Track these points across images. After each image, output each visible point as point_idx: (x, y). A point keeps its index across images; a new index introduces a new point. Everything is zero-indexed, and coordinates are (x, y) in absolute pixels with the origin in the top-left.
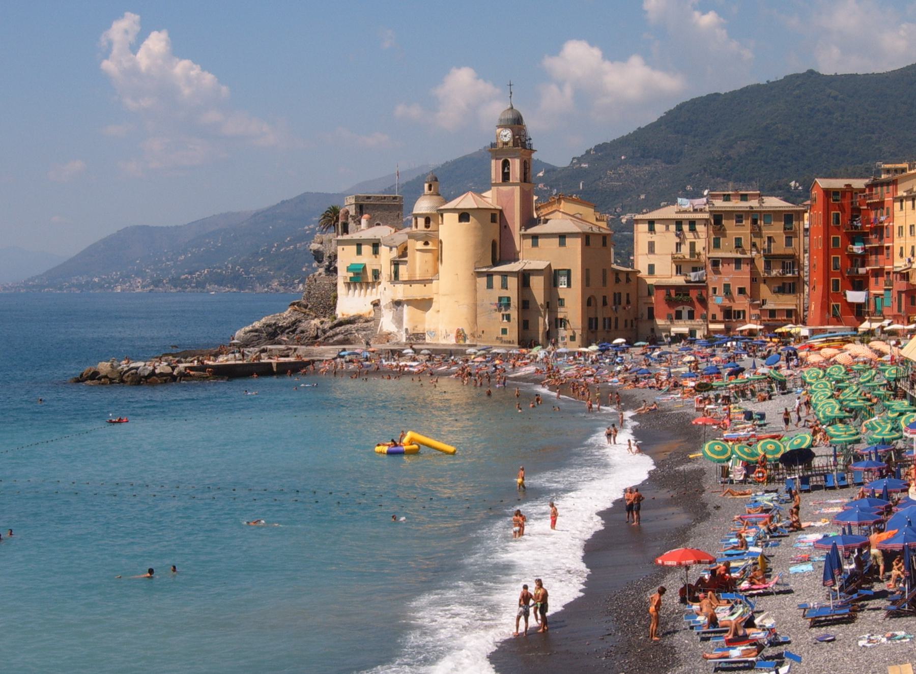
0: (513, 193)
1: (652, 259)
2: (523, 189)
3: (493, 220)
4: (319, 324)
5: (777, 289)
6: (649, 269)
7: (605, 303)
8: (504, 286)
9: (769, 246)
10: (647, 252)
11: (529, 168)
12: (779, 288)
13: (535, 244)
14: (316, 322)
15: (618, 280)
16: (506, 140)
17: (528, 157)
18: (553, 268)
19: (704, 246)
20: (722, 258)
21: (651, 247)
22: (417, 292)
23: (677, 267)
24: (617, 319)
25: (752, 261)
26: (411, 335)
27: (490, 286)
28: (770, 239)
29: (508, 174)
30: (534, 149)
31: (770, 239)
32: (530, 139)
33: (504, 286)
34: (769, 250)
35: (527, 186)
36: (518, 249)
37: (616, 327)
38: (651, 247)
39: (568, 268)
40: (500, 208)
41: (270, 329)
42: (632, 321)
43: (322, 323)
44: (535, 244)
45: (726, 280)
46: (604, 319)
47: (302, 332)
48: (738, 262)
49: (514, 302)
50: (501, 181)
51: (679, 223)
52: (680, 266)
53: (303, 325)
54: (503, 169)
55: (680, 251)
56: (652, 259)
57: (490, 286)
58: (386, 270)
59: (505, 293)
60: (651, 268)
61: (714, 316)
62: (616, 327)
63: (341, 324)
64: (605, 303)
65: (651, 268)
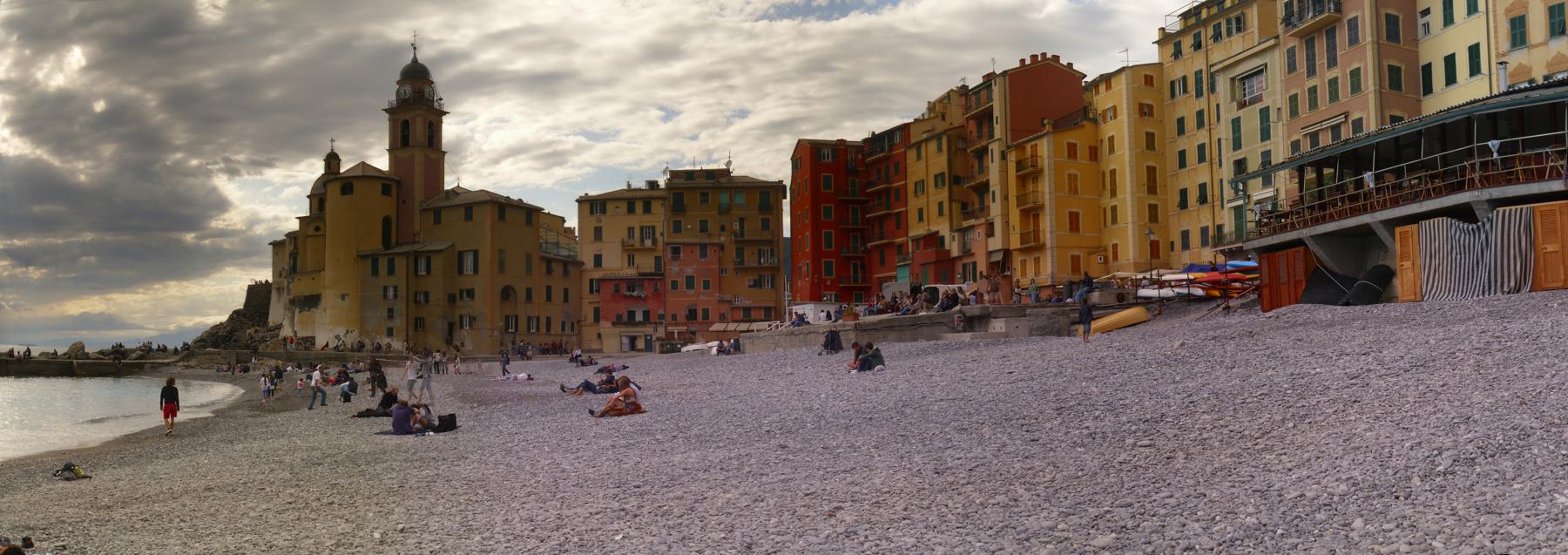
3: (386, 190)
5: (752, 283)
7: (529, 297)
8: (391, 271)
9: (742, 226)
10: (593, 239)
12: (755, 281)
13: (437, 220)
15: (549, 271)
20: (683, 244)
25: (722, 247)
27: (375, 272)
32: (441, 99)
33: (391, 271)
34: (742, 234)
36: (417, 228)
39: (474, 248)
40: (398, 179)
42: (573, 324)
45: (690, 271)
46: (529, 319)
48: (703, 247)
50: (399, 146)
54: (403, 131)
57: (375, 272)
60: (598, 260)
61: (674, 317)
64: (529, 297)
65: (598, 260)
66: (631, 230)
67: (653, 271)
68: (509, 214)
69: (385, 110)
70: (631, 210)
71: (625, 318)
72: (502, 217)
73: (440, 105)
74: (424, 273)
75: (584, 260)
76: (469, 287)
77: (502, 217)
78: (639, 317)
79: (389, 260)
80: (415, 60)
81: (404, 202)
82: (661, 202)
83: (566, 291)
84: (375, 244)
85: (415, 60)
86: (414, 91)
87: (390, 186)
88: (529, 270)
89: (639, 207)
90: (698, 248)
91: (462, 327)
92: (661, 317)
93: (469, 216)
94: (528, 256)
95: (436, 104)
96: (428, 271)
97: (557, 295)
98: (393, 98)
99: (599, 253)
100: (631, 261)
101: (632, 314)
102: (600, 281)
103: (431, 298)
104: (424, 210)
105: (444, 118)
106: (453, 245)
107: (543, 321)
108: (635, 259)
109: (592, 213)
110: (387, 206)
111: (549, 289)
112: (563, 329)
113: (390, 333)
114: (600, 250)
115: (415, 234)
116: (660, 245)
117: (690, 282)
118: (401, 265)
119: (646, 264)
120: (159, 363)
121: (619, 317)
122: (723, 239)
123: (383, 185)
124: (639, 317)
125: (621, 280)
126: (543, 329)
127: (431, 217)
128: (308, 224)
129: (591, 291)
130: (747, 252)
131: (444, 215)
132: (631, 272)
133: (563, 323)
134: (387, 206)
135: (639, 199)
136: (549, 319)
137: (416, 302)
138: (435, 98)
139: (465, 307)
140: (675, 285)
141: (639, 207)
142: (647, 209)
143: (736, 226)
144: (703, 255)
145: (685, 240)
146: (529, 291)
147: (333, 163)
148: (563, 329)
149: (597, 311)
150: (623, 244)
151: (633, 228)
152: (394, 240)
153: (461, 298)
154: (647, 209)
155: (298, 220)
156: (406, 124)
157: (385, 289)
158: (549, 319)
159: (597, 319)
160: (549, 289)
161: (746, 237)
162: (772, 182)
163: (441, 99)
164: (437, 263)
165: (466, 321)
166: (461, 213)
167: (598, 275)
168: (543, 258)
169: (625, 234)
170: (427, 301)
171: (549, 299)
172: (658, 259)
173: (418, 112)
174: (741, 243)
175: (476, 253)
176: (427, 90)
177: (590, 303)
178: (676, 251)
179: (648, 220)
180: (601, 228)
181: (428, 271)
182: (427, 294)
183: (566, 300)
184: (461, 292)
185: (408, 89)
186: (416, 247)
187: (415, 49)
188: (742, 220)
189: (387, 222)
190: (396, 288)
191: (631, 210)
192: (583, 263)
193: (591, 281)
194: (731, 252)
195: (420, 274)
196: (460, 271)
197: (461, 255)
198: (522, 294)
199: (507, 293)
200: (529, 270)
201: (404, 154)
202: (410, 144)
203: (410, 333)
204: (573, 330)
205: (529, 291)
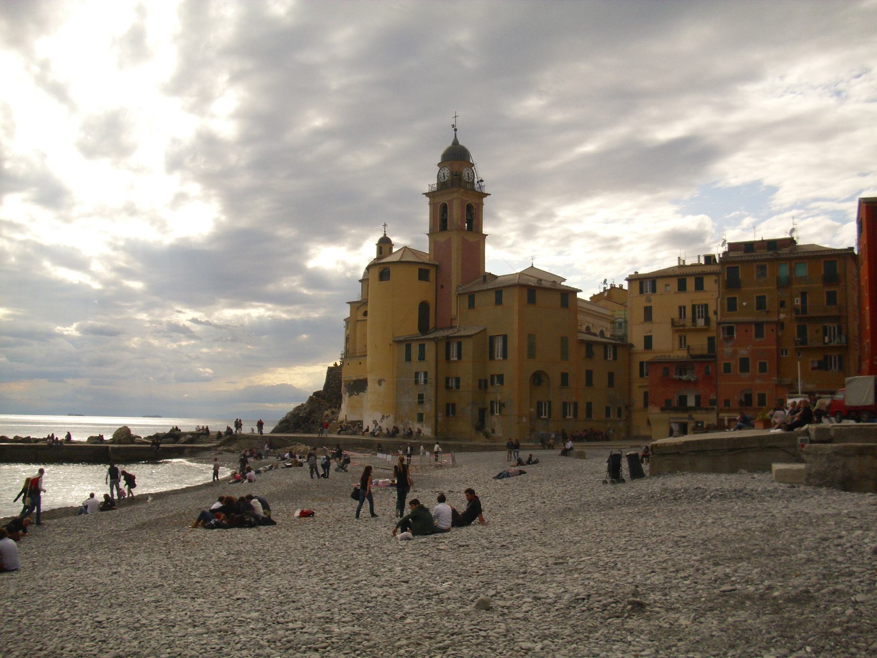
2: (463, 238)
3: (423, 275)
5: (816, 365)
6: (645, 341)
8: (422, 357)
9: (804, 301)
10: (642, 319)
11: (475, 214)
12: (819, 362)
13: (472, 305)
15: (590, 354)
17: (477, 202)
19: (715, 309)
20: (736, 323)
23: (680, 337)
25: (781, 325)
26: (349, 423)
27: (408, 358)
30: (486, 192)
32: (482, 181)
33: (422, 357)
34: (804, 309)
35: (471, 238)
38: (648, 313)
40: (437, 263)
42: (619, 410)
45: (744, 352)
46: (565, 404)
48: (759, 326)
49: (432, 375)
52: (685, 338)
55: (685, 317)
57: (408, 358)
59: (422, 367)
60: (648, 342)
61: (727, 403)
65: (648, 342)
66: (682, 309)
67: (705, 352)
68: (540, 297)
69: (427, 194)
71: (675, 403)
72: (532, 300)
73: (480, 187)
74: (456, 359)
75: (634, 343)
76: (498, 371)
77: (532, 300)
78: (691, 402)
79: (406, 345)
80: (456, 142)
81: (442, 287)
82: (714, 278)
83: (611, 376)
84: (411, 327)
85: (456, 142)
86: (452, 173)
87: (427, 271)
88: (565, 354)
89: (691, 283)
90: (753, 327)
91: (492, 412)
92: (713, 402)
93: (499, 301)
94: (564, 341)
95: (476, 186)
96: (459, 356)
97: (600, 379)
98: (435, 181)
99: (649, 334)
100: (682, 341)
101: (683, 399)
102: (650, 363)
103: (462, 383)
104: (459, 294)
105: (485, 200)
106: (485, 330)
107: (582, 406)
108: (687, 339)
109: (641, 291)
110: (424, 291)
111: (589, 374)
112: (608, 414)
113: (420, 418)
114: (650, 331)
115: (451, 319)
116: (713, 325)
117: (744, 364)
118: (430, 350)
119: (699, 343)
120: (198, 448)
121: (668, 402)
122: (782, 316)
123: (420, 270)
124: (691, 402)
125: (671, 362)
126: (582, 414)
127: (466, 299)
128: (358, 308)
129: (642, 374)
131: (478, 300)
132: (682, 354)
133: (608, 410)
134: (424, 291)
135: (691, 275)
136: (589, 406)
137: (448, 387)
138: (476, 180)
139: (497, 393)
140: (727, 367)
141: (691, 283)
142: (699, 286)
143: (798, 301)
144: (759, 334)
145: (741, 319)
146: (565, 377)
147: (385, 248)
148: (608, 414)
149: (646, 395)
150: (673, 323)
151: (685, 308)
152: (431, 326)
153: (492, 383)
154: (699, 286)
155: (349, 306)
156: (444, 207)
157: (417, 374)
158: (589, 406)
159: (646, 405)
160: (589, 374)
161: (809, 314)
162: (841, 250)
163: (482, 181)
164: (468, 347)
165: (496, 408)
166: (492, 297)
167: (648, 357)
168: (582, 342)
169: (676, 315)
170: (458, 387)
172: (711, 340)
173: (455, 195)
175: (505, 338)
176: (465, 172)
177: (640, 387)
178: (730, 330)
179: (700, 298)
180: (651, 307)
181: (459, 356)
182: (458, 380)
183: (611, 383)
184: (492, 376)
185: (446, 171)
186: (446, 333)
187: (456, 130)
188: (804, 295)
189: (424, 308)
190: (426, 374)
191: (682, 287)
192: (632, 346)
193: (641, 364)
195: (452, 359)
196: (492, 357)
197: (492, 339)
198: (556, 379)
199: (538, 379)
201: (442, 238)
202: (448, 228)
203: (440, 419)
204: (619, 415)
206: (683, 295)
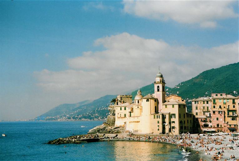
0: (160, 94)
1: (197, 111)
3: (155, 101)
4: (110, 128)
9: (229, 107)
13: (166, 107)
14: (110, 127)
16: (158, 81)
18: (171, 113)
21: (197, 108)
22: (136, 119)
24: (188, 127)
27: (155, 118)
28: (229, 106)
29: (159, 89)
31: (229, 106)
34: (229, 109)
35: (164, 93)
37: (188, 129)
38: (197, 108)
41: (98, 130)
43: (111, 128)
44: (166, 107)
47: (106, 130)
51: (204, 101)
53: (107, 128)
56: (197, 111)
58: (128, 114)
60: (197, 114)
61: (214, 126)
62: (188, 129)
63: (116, 128)
64: (184, 123)
65: (197, 114)
66: (204, 107)
68: (181, 106)
70: (204, 103)
88: (184, 117)
107: (187, 127)
111: (188, 120)
130: (230, 113)
141: (206, 102)
142: (207, 103)
146: (185, 121)
154: (207, 103)
160: (188, 120)
171: (188, 122)
174: (229, 111)
189: (156, 107)
194: (226, 112)
200: (184, 117)
205: (185, 121)
206: (204, 104)
